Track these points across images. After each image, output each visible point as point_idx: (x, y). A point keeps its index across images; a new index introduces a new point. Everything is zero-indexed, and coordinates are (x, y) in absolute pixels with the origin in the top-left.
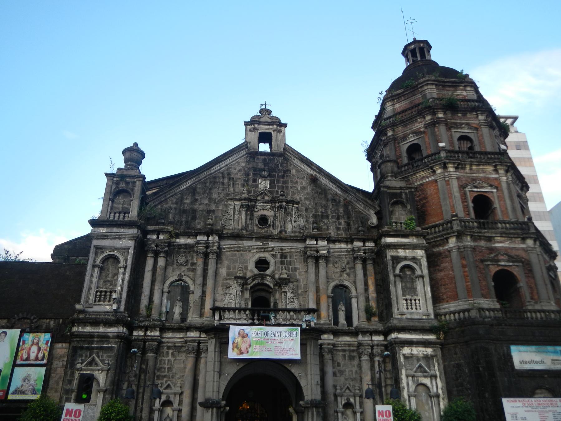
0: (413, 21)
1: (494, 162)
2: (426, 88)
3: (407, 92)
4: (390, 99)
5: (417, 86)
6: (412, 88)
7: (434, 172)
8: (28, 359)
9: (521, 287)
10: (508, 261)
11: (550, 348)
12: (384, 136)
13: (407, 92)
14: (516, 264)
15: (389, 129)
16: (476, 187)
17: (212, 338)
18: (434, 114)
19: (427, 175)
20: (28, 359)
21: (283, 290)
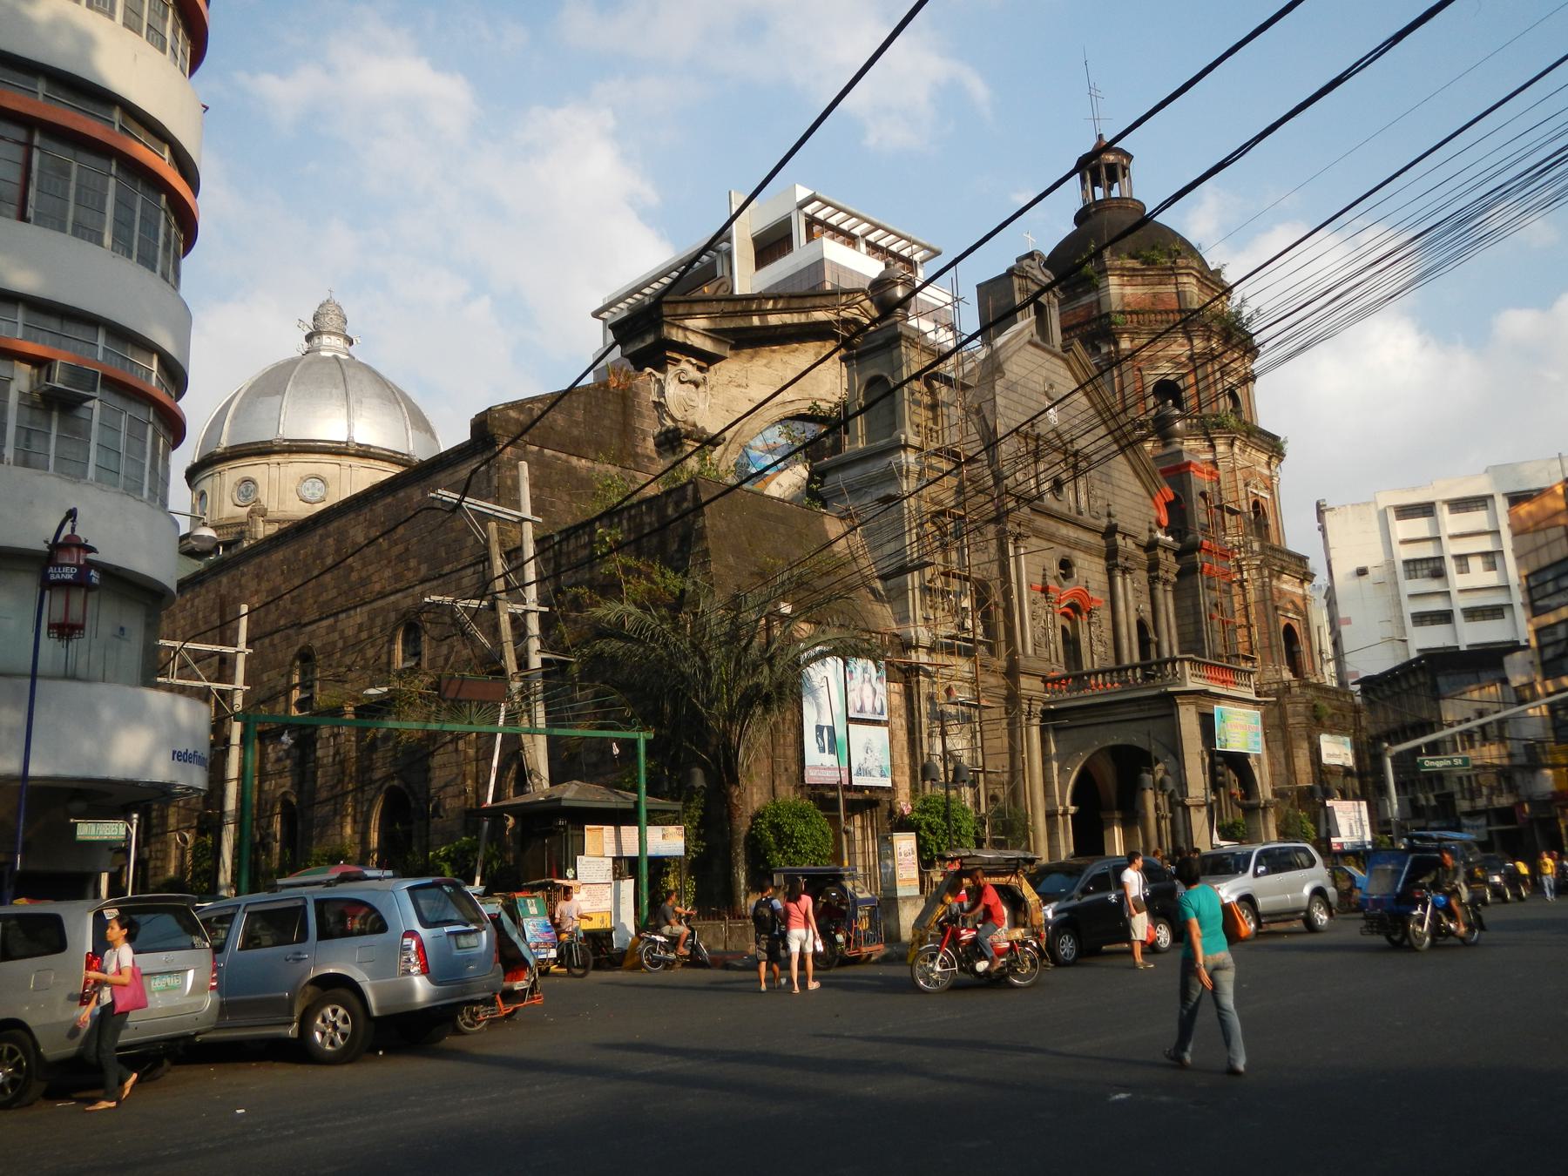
0: (1098, 94)
1: (1273, 451)
2: (1185, 279)
3: (1150, 273)
4: (1118, 272)
5: (1171, 269)
6: (1162, 269)
7: (1213, 447)
8: (862, 710)
9: (1300, 651)
10: (1295, 613)
11: (1341, 739)
12: (1109, 344)
13: (1150, 273)
14: (1299, 618)
15: (1125, 335)
16: (1256, 488)
17: (1190, 703)
18: (1209, 339)
19: (1199, 447)
20: (862, 710)
21: (1094, 620)
